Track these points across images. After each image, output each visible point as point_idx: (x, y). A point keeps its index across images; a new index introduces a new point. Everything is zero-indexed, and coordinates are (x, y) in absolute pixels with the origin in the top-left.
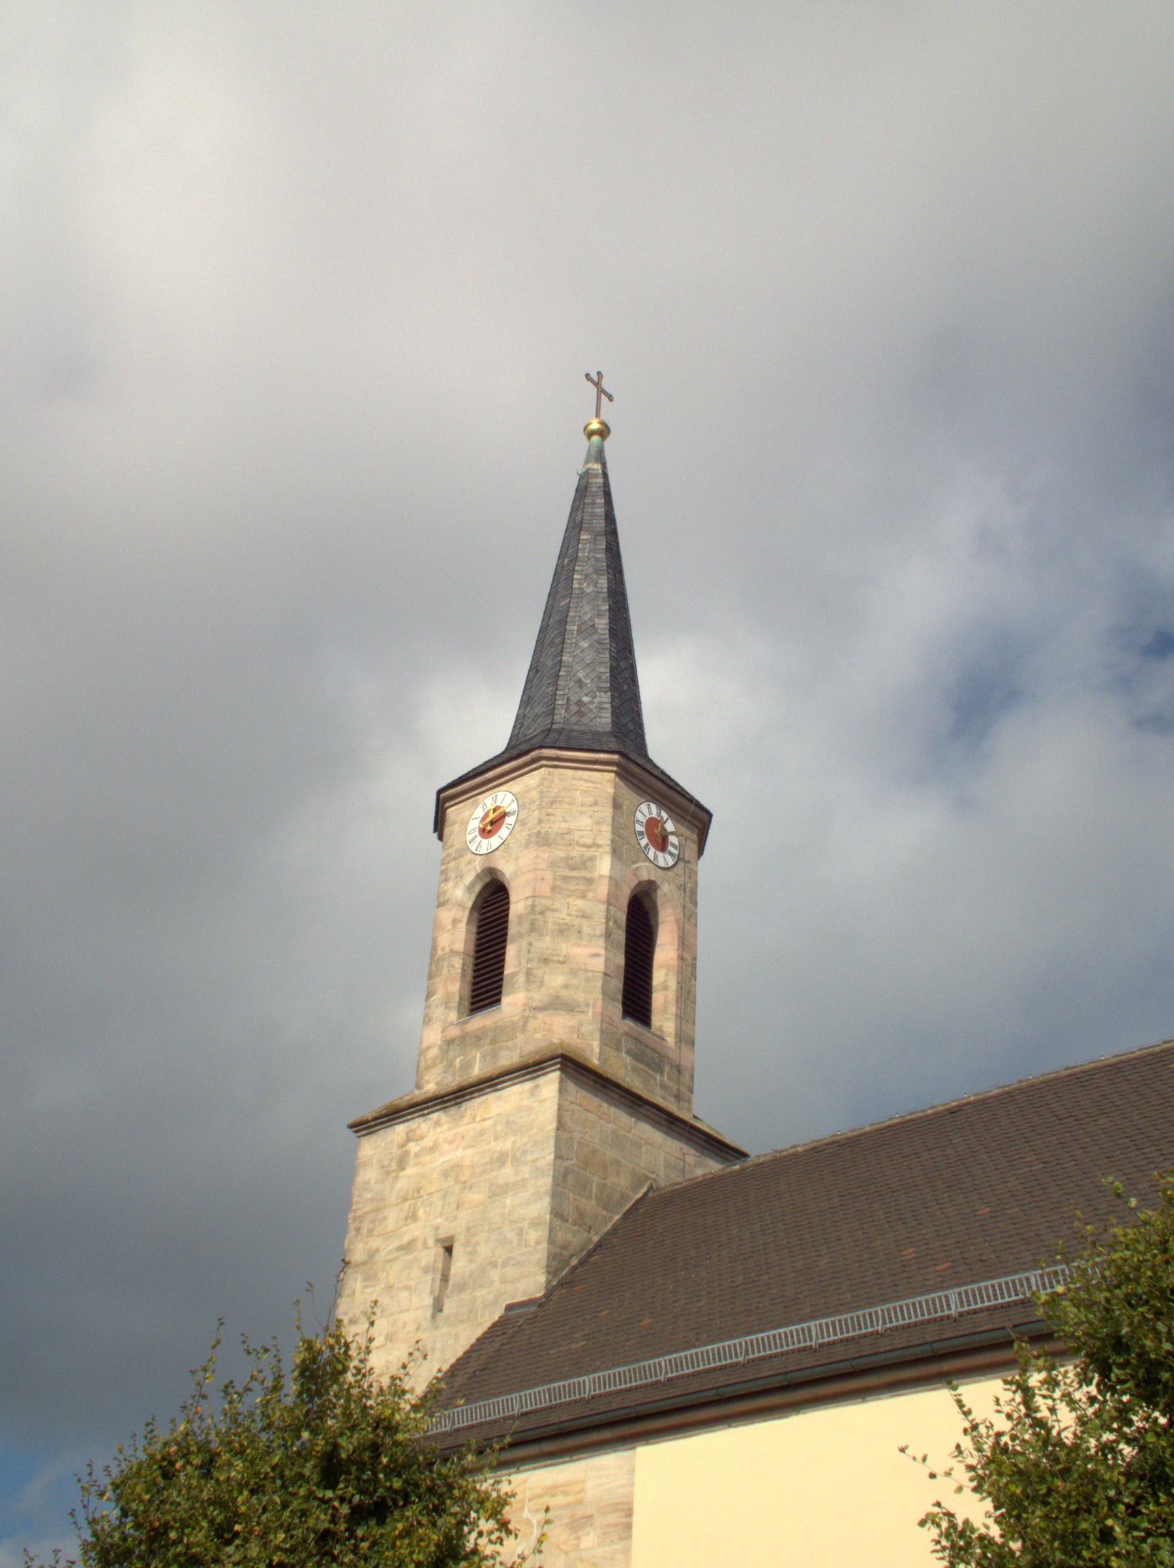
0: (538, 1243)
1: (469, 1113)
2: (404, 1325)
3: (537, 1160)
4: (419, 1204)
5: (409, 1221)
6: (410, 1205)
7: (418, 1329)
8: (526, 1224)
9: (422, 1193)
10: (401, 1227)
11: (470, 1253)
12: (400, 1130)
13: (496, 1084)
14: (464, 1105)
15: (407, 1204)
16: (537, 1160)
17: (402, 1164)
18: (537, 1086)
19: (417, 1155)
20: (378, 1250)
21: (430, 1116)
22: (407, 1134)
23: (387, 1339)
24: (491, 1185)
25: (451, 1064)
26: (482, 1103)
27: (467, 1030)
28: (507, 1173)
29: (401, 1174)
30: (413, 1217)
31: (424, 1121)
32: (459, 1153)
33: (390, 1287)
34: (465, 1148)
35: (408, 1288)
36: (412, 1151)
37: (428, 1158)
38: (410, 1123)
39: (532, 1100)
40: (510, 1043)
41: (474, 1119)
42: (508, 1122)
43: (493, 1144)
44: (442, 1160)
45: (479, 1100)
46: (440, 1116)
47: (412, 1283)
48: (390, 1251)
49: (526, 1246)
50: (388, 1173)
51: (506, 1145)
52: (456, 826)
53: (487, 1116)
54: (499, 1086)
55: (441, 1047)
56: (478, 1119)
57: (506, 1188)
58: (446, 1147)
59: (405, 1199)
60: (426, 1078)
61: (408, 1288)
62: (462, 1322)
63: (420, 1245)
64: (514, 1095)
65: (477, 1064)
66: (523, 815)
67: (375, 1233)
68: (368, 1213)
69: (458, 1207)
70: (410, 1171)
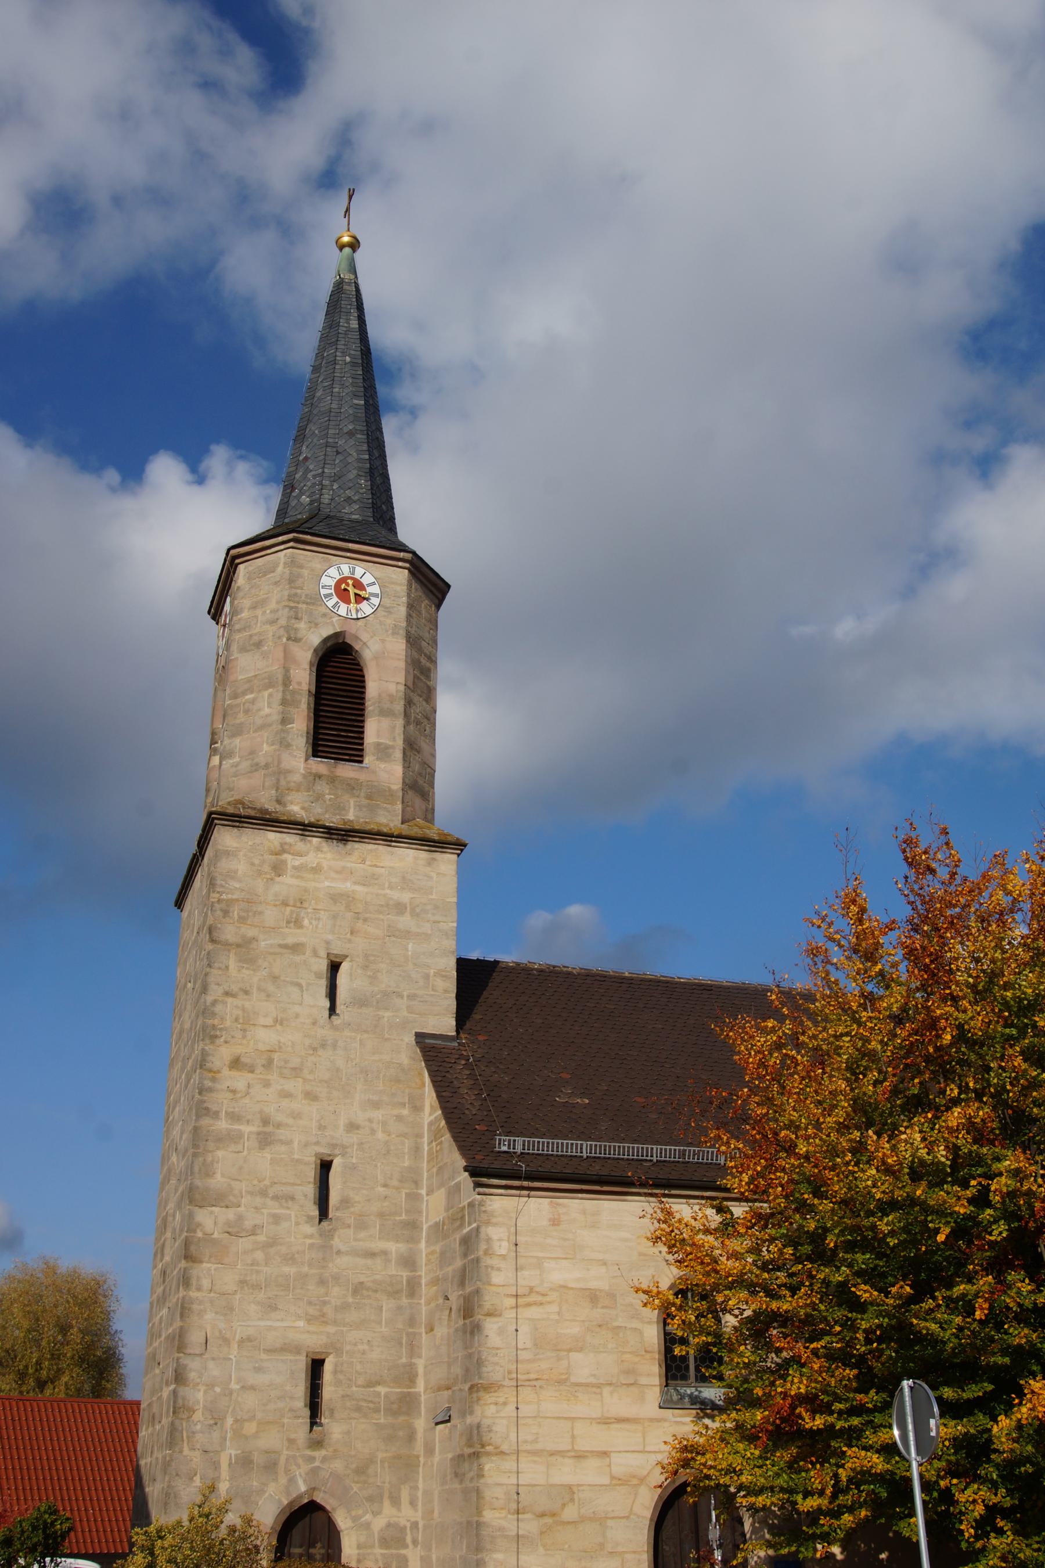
0: (446, 991)
1: (356, 853)
2: (297, 1016)
3: (439, 922)
4: (302, 915)
5: (292, 925)
6: (292, 912)
7: (314, 1024)
8: (432, 971)
9: (305, 905)
10: (282, 928)
11: (369, 977)
12: (273, 838)
13: (391, 841)
14: (350, 845)
15: (289, 909)
16: (439, 922)
17: (278, 869)
18: (434, 859)
19: (295, 868)
20: (254, 939)
21: (309, 838)
22: (282, 845)
23: (276, 1021)
24: (389, 926)
25: (319, 797)
26: (371, 850)
27: (338, 774)
28: (405, 921)
29: (277, 879)
30: (298, 923)
31: (302, 840)
32: (348, 886)
33: (275, 978)
34: (355, 883)
35: (299, 985)
36: (289, 862)
37: (311, 876)
38: (284, 835)
39: (429, 869)
40: (388, 806)
41: (363, 861)
42: (404, 878)
43: (388, 891)
44: (327, 884)
45: (371, 846)
46: (320, 843)
47: (304, 983)
48: (271, 945)
49: (433, 990)
50: (260, 873)
51: (405, 897)
52: (305, 572)
53: (378, 864)
54: (393, 844)
55: (304, 776)
56: (367, 863)
57: (407, 934)
58: (333, 875)
59: (285, 904)
60: (289, 798)
61: (299, 985)
62: (366, 1032)
63: (308, 953)
64: (408, 857)
65: (352, 810)
66: (387, 602)
67: (249, 922)
68: (237, 900)
69: (352, 933)
70: (288, 880)
